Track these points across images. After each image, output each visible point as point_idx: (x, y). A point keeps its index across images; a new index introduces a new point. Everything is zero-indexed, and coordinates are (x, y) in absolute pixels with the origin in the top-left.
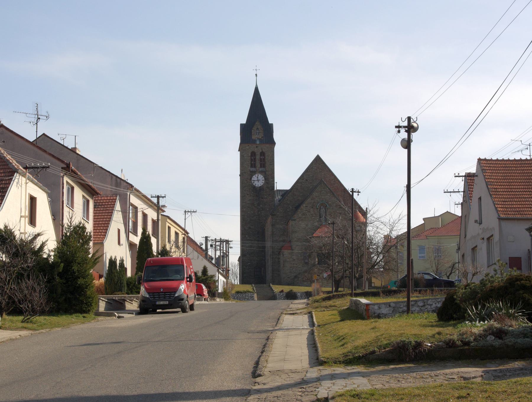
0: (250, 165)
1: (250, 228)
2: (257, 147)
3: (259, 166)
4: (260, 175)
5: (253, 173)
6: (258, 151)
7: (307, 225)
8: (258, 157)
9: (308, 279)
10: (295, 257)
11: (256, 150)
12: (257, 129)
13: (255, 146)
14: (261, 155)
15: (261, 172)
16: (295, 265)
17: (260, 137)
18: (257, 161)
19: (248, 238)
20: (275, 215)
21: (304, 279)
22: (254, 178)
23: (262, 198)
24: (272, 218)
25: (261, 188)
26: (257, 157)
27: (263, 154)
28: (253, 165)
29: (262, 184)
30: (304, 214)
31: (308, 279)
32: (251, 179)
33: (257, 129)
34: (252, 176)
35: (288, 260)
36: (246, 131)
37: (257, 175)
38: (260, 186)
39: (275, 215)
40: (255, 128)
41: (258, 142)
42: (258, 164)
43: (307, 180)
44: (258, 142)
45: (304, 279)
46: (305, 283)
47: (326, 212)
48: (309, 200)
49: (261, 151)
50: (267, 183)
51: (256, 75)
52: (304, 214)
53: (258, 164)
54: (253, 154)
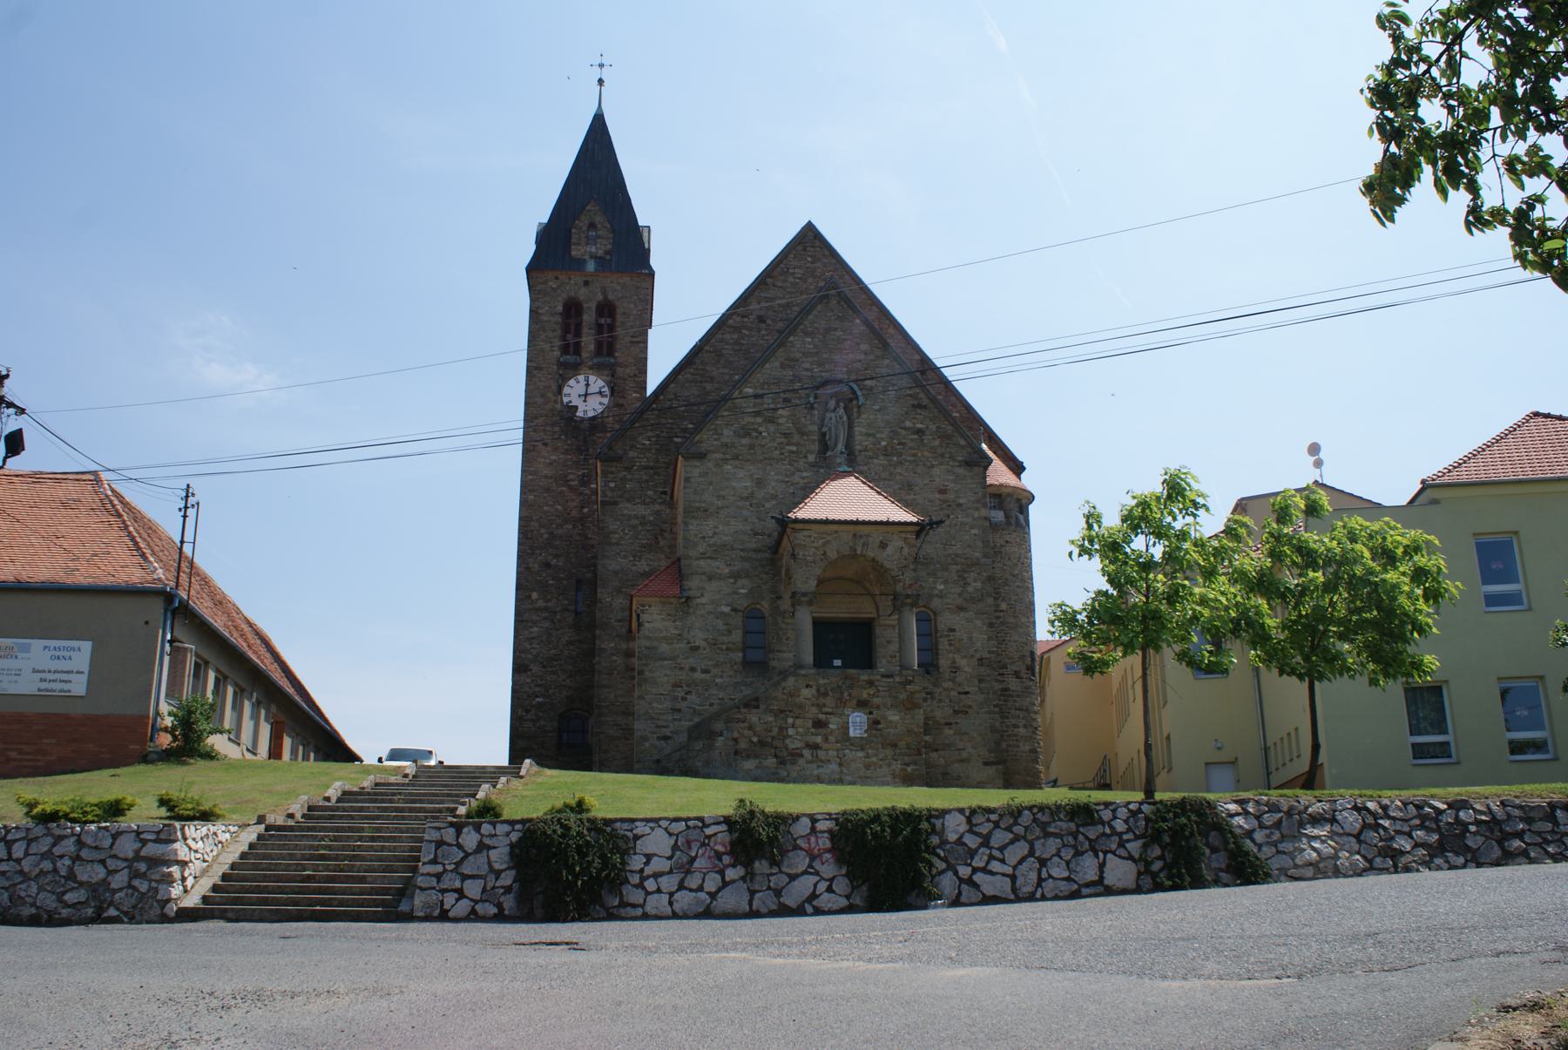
0: (558, 343)
1: (547, 565)
2: (586, 283)
3: (592, 347)
4: (592, 378)
5: (569, 369)
7: (760, 483)
8: (589, 317)
9: (762, 743)
10: (699, 637)
11: (582, 294)
12: (592, 226)
13: (577, 279)
15: (598, 369)
16: (698, 675)
17: (601, 253)
18: (585, 330)
19: (541, 604)
20: (619, 459)
21: (743, 745)
22: (573, 391)
25: (595, 423)
26: (585, 317)
27: (606, 309)
28: (571, 347)
29: (600, 409)
31: (762, 743)
32: (560, 391)
33: (592, 226)
35: (664, 648)
37: (581, 378)
38: (591, 414)
39: (619, 459)
40: (582, 223)
41: (591, 266)
42: (588, 341)
43: (761, 319)
44: (591, 266)
45: (743, 745)
46: (749, 764)
47: (850, 427)
48: (772, 368)
49: (600, 297)
50: (620, 406)
51: (601, 82)
53: (588, 341)
54: (572, 309)
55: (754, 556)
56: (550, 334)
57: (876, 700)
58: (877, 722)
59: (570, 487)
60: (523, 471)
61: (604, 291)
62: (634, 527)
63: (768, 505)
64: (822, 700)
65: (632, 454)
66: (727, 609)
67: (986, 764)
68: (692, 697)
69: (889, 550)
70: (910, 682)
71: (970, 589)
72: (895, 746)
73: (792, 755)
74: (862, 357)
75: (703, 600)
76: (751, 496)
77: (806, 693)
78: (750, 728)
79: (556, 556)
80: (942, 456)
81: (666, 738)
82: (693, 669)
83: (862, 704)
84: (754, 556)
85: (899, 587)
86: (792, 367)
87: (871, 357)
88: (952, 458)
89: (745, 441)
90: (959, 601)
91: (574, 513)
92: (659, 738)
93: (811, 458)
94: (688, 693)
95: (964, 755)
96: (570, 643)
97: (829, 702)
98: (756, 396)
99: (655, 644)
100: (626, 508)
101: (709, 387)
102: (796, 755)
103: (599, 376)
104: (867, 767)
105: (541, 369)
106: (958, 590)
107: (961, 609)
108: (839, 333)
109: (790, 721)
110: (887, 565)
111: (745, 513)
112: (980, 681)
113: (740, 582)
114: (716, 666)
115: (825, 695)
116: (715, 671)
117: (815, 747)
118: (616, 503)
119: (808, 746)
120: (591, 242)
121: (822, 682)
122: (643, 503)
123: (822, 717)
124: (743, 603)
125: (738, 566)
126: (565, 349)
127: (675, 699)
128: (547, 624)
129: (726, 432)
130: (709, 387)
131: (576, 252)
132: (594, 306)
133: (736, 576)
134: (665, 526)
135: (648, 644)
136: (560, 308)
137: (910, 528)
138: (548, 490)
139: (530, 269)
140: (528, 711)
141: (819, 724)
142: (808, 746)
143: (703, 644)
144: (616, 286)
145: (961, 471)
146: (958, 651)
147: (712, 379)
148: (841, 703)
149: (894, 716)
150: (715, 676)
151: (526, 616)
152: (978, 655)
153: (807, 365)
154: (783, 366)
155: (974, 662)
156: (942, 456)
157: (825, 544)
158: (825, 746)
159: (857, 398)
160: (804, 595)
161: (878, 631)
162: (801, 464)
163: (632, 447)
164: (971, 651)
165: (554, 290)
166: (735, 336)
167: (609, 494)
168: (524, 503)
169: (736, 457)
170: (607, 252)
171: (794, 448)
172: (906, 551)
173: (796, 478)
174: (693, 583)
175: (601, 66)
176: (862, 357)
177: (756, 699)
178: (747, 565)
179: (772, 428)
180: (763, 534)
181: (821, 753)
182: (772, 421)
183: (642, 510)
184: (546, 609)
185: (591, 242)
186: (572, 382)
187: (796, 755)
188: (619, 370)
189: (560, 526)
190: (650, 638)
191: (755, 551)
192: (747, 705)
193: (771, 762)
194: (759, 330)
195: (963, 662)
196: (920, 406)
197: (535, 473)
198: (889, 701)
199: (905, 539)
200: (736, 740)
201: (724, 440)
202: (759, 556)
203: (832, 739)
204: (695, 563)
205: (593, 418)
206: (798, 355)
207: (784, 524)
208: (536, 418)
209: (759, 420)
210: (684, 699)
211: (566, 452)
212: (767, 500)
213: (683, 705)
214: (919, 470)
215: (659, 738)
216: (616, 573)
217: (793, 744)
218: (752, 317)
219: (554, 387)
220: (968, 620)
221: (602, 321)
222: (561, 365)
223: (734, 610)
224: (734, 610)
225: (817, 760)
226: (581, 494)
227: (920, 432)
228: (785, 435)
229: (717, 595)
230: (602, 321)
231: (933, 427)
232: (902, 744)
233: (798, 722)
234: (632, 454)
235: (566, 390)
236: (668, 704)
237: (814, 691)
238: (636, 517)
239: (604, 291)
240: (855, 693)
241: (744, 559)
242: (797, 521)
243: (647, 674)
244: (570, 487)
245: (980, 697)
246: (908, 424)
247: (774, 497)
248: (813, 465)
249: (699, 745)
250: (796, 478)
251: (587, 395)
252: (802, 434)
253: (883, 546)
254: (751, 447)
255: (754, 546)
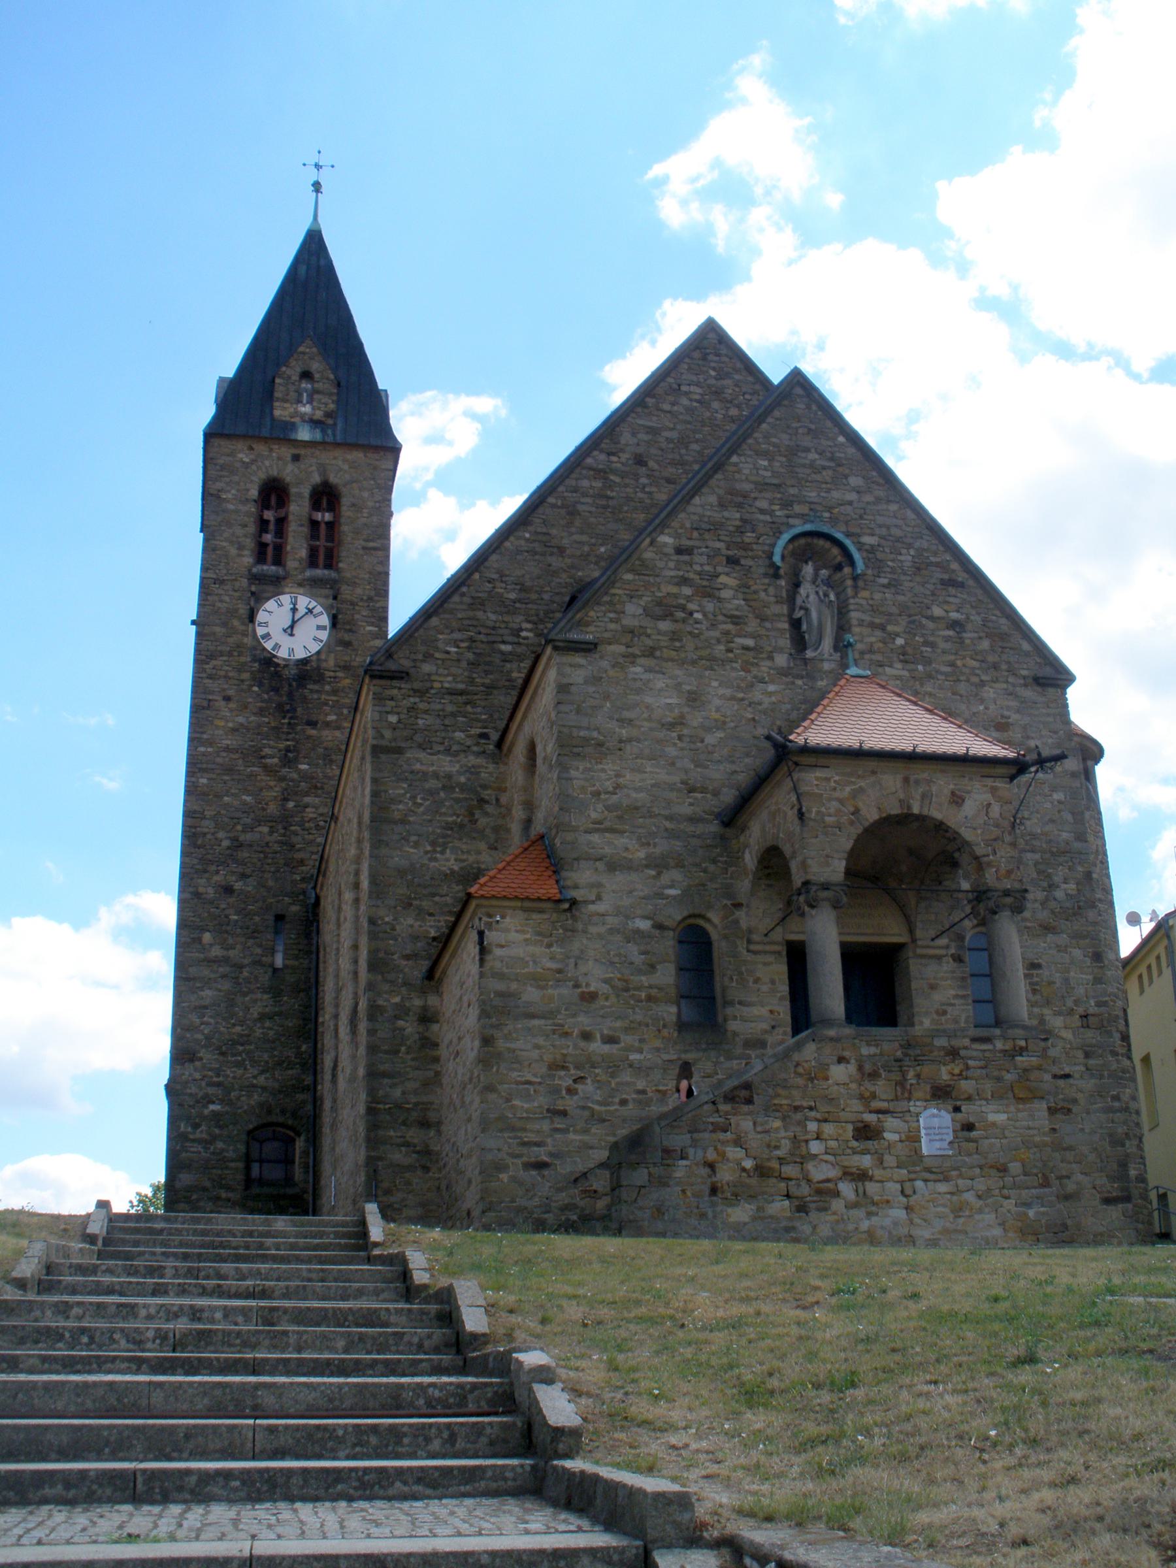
1: (228, 890)
2: (296, 458)
3: (303, 553)
4: (303, 602)
5: (264, 586)
6: (300, 480)
7: (694, 699)
8: (298, 508)
10: (595, 976)
13: (287, 452)
14: (316, 505)
15: (312, 586)
17: (319, 415)
19: (216, 952)
20: (401, 675)
21: (725, 1175)
22: (273, 617)
23: (312, 724)
24: (379, 699)
26: (293, 508)
27: (326, 496)
28: (270, 550)
29: (315, 648)
30: (664, 609)
31: (762, 1171)
32: (252, 618)
34: (259, 599)
35: (531, 994)
36: (243, 411)
37: (286, 599)
38: (300, 654)
39: (401, 675)
40: (292, 370)
42: (297, 547)
43: (640, 461)
44: (304, 434)
46: (740, 1213)
47: (842, 612)
48: (705, 504)
49: (317, 479)
50: (347, 644)
51: (317, 187)
52: (664, 609)
53: (297, 547)
55: (690, 828)
56: (239, 531)
57: (967, 1086)
58: (969, 1127)
59: (265, 767)
60: (191, 740)
61: (322, 469)
62: (431, 793)
63: (710, 739)
64: (869, 1086)
65: (427, 668)
66: (644, 925)
67: (1108, 1201)
68: (587, 1088)
69: (970, 807)
70: (1021, 1051)
71: (1059, 894)
72: (1003, 1170)
73: (819, 1192)
74: (853, 496)
75: (600, 907)
76: (680, 722)
77: (839, 1072)
78: (738, 1142)
79: (243, 876)
80: (995, 667)
81: (540, 1166)
82: (587, 1036)
83: (941, 1094)
84: (690, 828)
85: (990, 877)
86: (740, 506)
87: (868, 498)
88: (1012, 671)
89: (665, 625)
90: (1043, 915)
91: (273, 809)
92: (529, 1166)
93: (781, 660)
94: (579, 1080)
95: (1071, 1187)
96: (263, 1017)
97: (882, 1088)
98: (679, 551)
99: (514, 986)
100: (420, 761)
101: (556, 562)
102: (826, 1192)
103: (312, 596)
104: (957, 1211)
105: (222, 582)
106: (1040, 895)
107: (1048, 929)
108: (813, 456)
109: (812, 1126)
110: (967, 834)
111: (672, 751)
112: (1087, 1055)
113: (666, 878)
114: (627, 1030)
115: (874, 1075)
116: (627, 1039)
117: (862, 1176)
118: (399, 751)
119: (847, 1174)
120: (300, 413)
121: (865, 1051)
122: (448, 751)
123: (871, 1118)
124: (675, 915)
125: (661, 847)
126: (261, 557)
127: (556, 1091)
128: (226, 985)
129: (630, 608)
130: (556, 562)
131: (281, 412)
132: (306, 491)
133: (659, 864)
134: (486, 794)
135: (500, 986)
136: (254, 493)
137: (1001, 770)
138: (230, 770)
139: (210, 436)
140: (196, 1126)
141: (865, 1132)
142: (847, 1174)
143: (605, 988)
144: (340, 467)
145: (1029, 693)
146: (1048, 1003)
147: (561, 550)
148: (903, 1091)
149: (997, 1116)
150: (629, 1049)
151: (193, 971)
152: (1081, 1010)
153: (763, 504)
154: (722, 505)
155: (1076, 1021)
156: (995, 667)
157: (855, 794)
158: (878, 1173)
159: (852, 563)
160: (825, 887)
161: (914, 966)
162: (765, 666)
163: (428, 657)
164: (1070, 1003)
165: (246, 465)
166: (598, 484)
167: (388, 734)
168: (191, 790)
169: (650, 652)
170: (328, 415)
171: (750, 642)
172: (996, 809)
173: (757, 695)
174: (582, 877)
175: (318, 166)
176: (853, 496)
177: (747, 1086)
178: (678, 845)
179: (710, 606)
180: (704, 790)
181: (872, 1188)
182: (708, 592)
183: (447, 765)
184: (226, 960)
185: (300, 413)
186: (271, 605)
187: (826, 1192)
188: (346, 591)
189: (249, 828)
190: (501, 976)
191: (692, 820)
192: (730, 1098)
193: (780, 1207)
194: (636, 477)
195: (1057, 1022)
196: (952, 583)
197: (210, 743)
198: (988, 1087)
199: (993, 790)
200: (711, 1166)
201: (627, 621)
202: (700, 829)
203: (890, 1160)
204: (584, 838)
205: (304, 662)
206: (747, 487)
207: (786, 757)
208: (212, 656)
209: (687, 591)
210: (571, 1091)
211: (261, 712)
212: (708, 730)
213: (569, 1103)
214: (962, 688)
215: (529, 1166)
216: (402, 873)
217: (820, 1172)
218: (624, 457)
219: (243, 610)
220: (1061, 949)
221: (318, 516)
222: (255, 578)
223: (659, 927)
224: (659, 927)
225: (864, 1202)
226: (283, 779)
227: (955, 625)
228: (736, 620)
229: (626, 898)
230: (318, 516)
231: (977, 619)
232: (1015, 1167)
233: (829, 1129)
234: (427, 668)
235: (261, 616)
236: (542, 1101)
237: (852, 1068)
238: (436, 775)
239: (322, 469)
240: (926, 1070)
241: (672, 834)
242: (807, 750)
243: (501, 1044)
244: (265, 767)
245: (1089, 1084)
246: (937, 611)
247: (721, 725)
248: (783, 672)
249: (640, 1176)
250: (757, 695)
251: (293, 627)
252: (763, 619)
253: (957, 800)
254: (675, 636)
255: (686, 810)
